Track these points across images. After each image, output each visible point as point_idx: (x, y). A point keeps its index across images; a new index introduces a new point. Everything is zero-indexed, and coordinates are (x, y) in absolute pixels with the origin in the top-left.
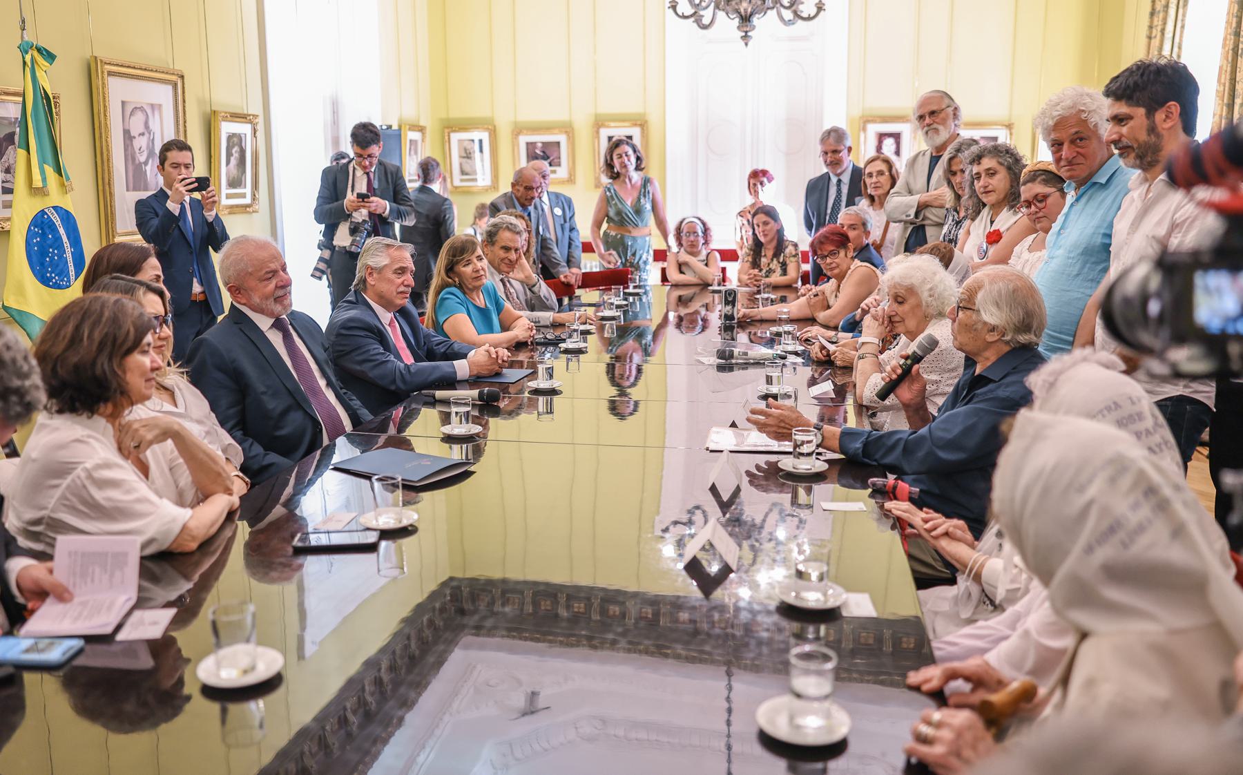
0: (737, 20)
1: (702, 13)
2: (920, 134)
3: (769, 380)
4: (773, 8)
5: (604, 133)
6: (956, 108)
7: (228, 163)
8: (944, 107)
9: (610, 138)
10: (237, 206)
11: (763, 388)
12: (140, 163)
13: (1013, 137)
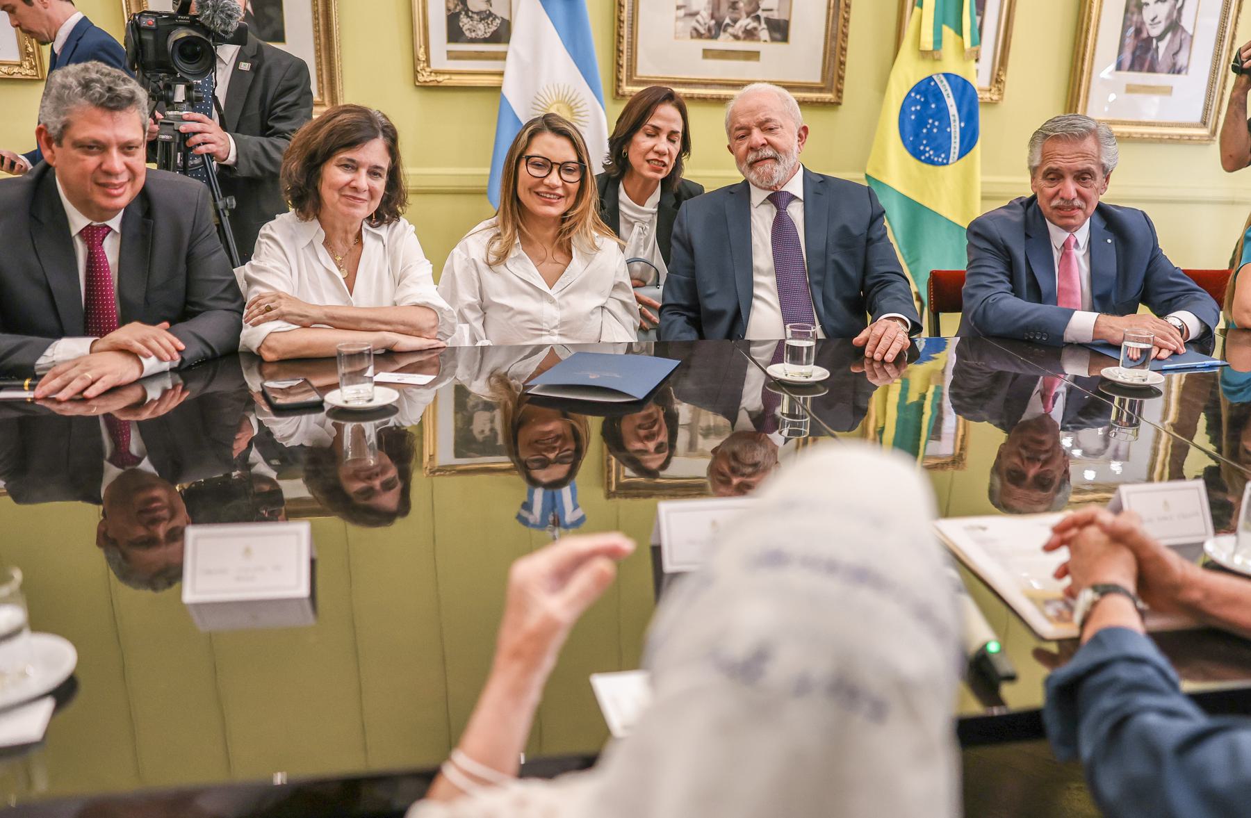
12: (1150, 39)
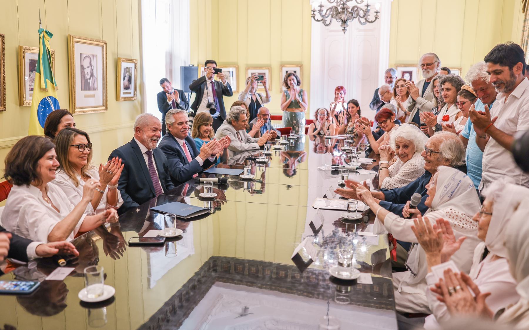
0: (341, 22)
1: (326, 19)
2: (421, 71)
3: (343, 178)
4: (356, 17)
5: (284, 70)
6: (439, 63)
7: (124, 79)
8: (434, 62)
9: (287, 72)
10: (127, 98)
11: (341, 181)
12: (87, 79)
13: (462, 74)
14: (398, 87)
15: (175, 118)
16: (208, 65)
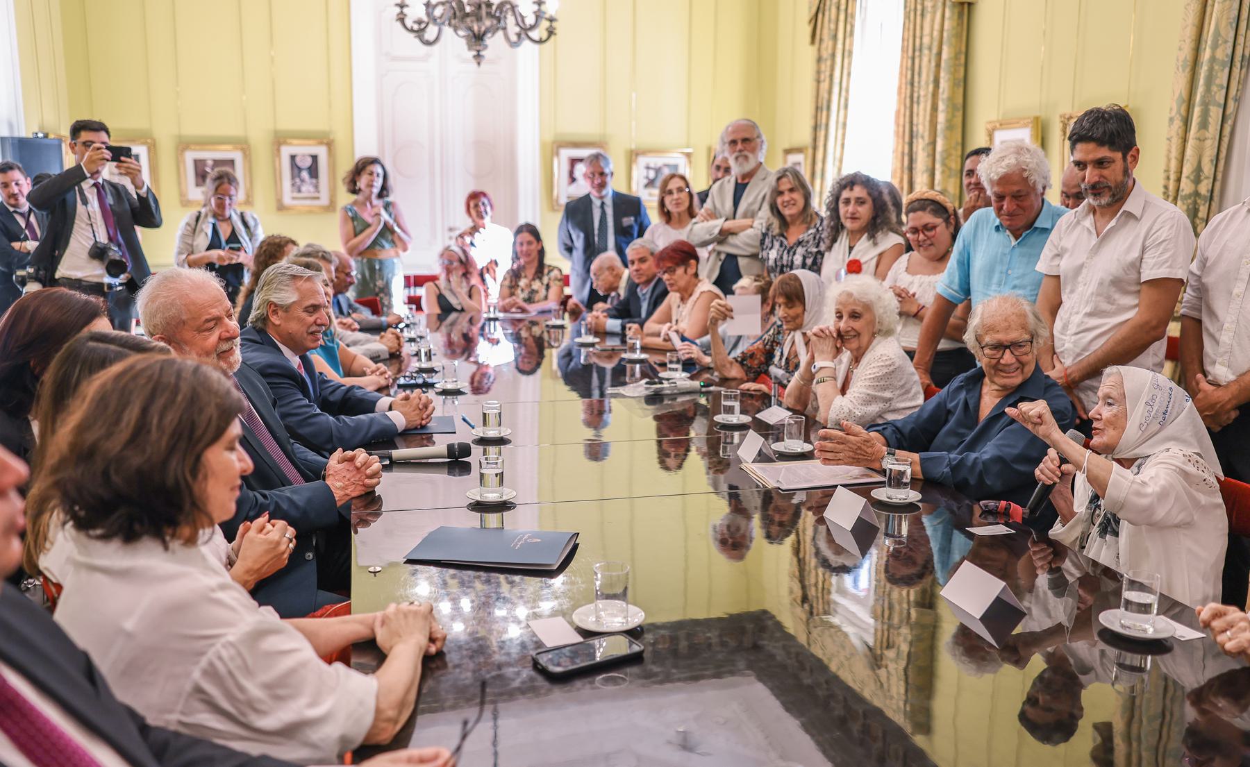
14: (670, 192)
15: (298, 289)
16: (85, 136)
